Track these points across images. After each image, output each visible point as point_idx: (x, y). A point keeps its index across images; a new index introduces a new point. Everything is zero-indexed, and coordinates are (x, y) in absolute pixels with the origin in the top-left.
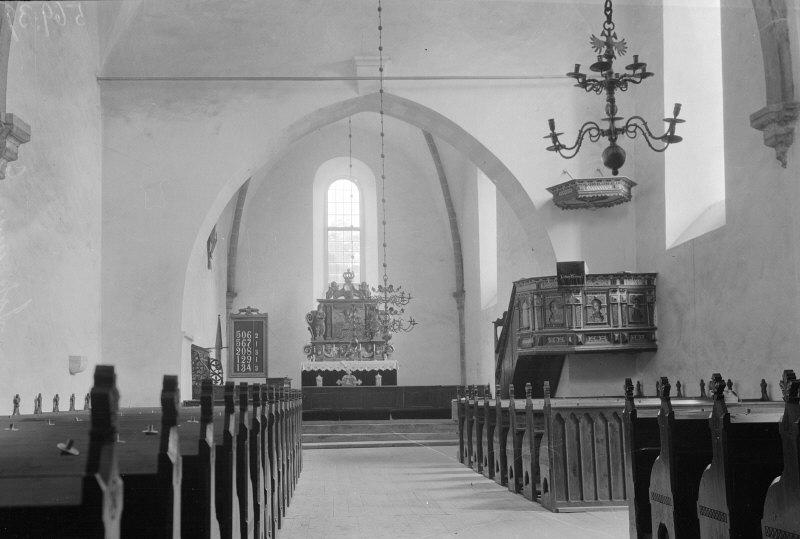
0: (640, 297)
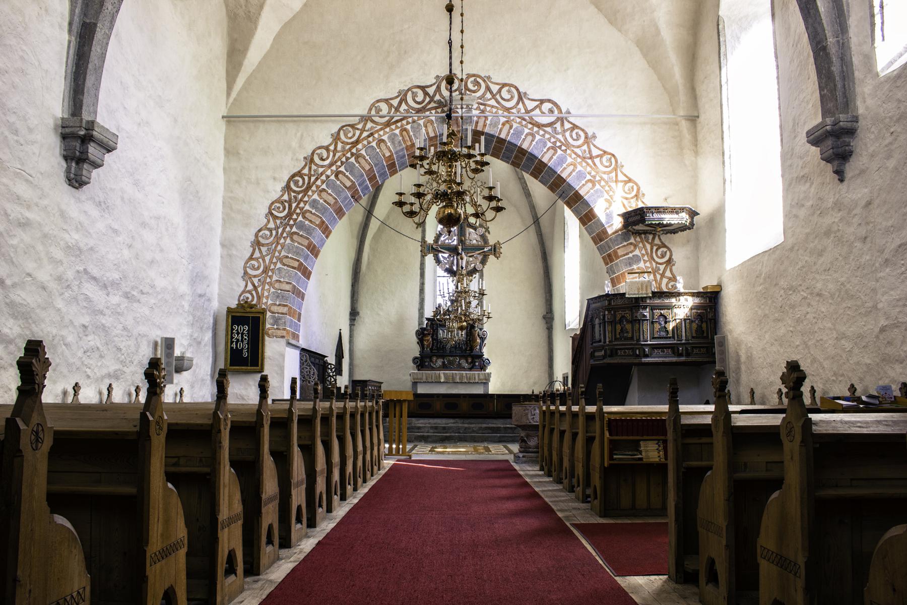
0: (701, 313)
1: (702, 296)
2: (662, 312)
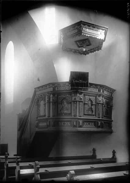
2: (90, 97)
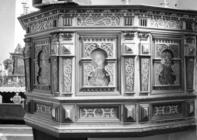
0: (172, 46)
1: (174, 19)
